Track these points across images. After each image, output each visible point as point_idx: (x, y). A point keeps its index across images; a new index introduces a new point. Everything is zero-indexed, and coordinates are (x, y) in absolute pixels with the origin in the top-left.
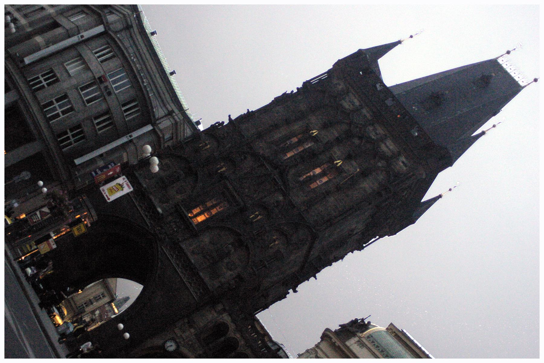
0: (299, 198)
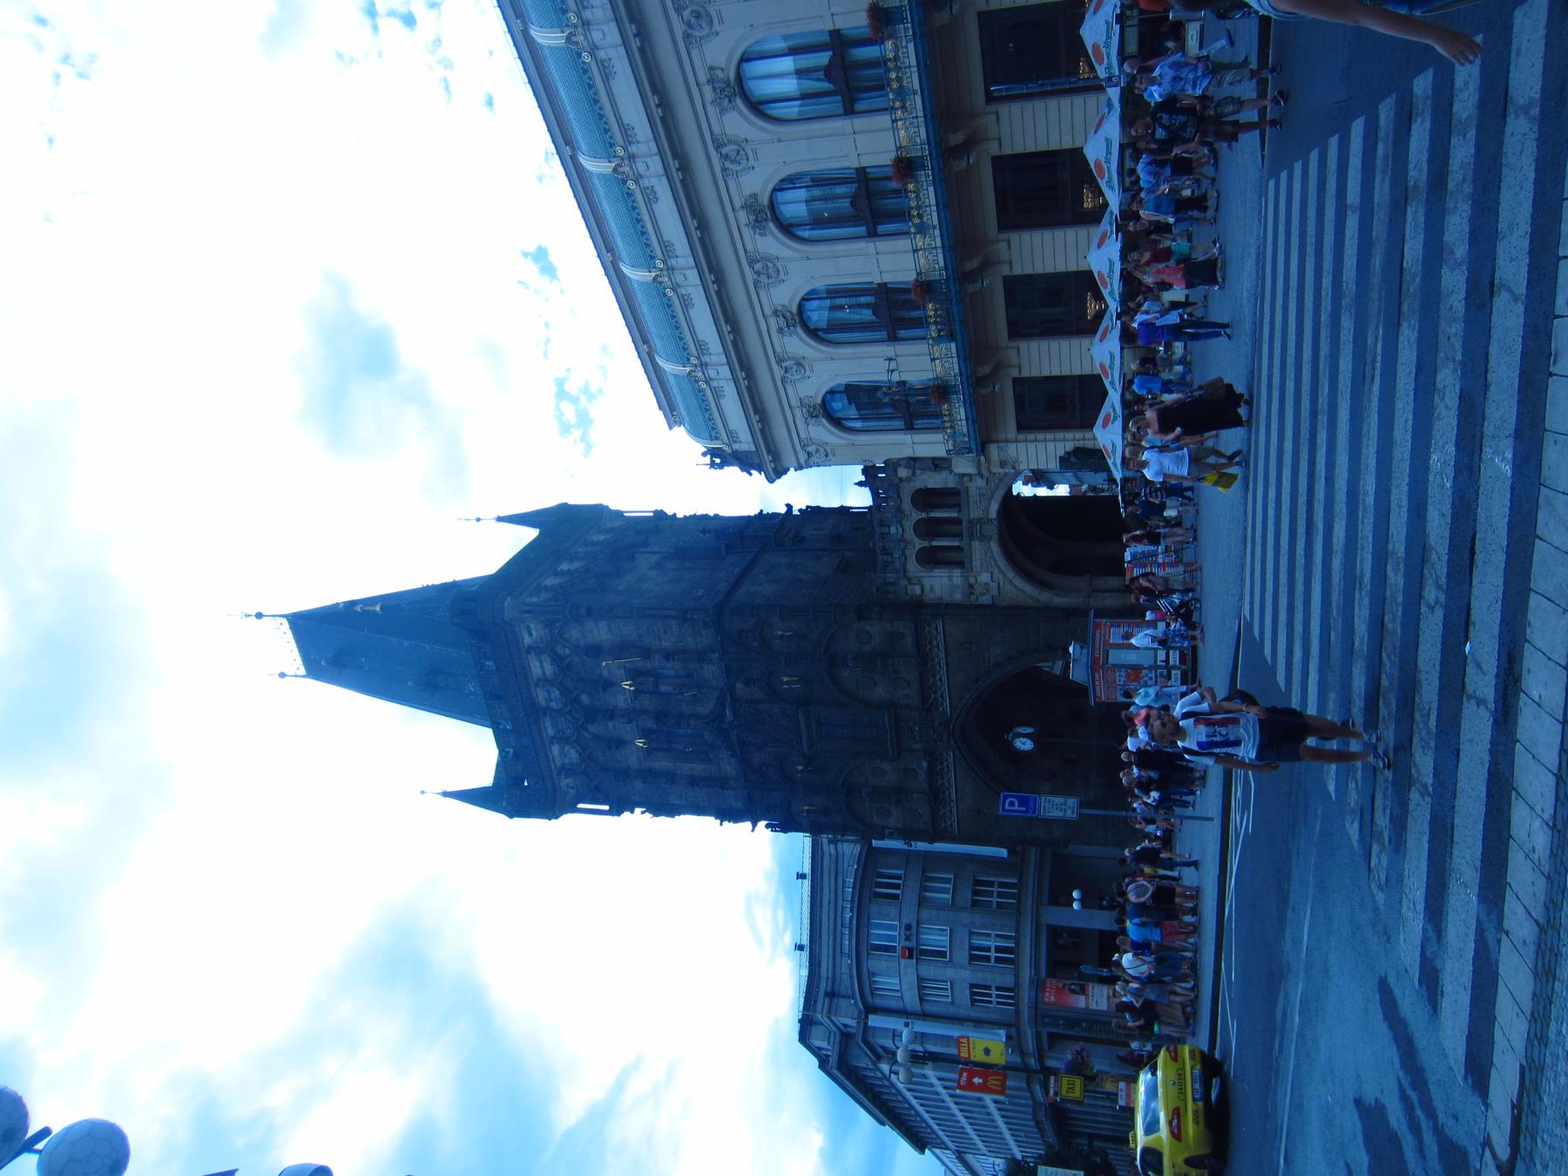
0: (711, 671)
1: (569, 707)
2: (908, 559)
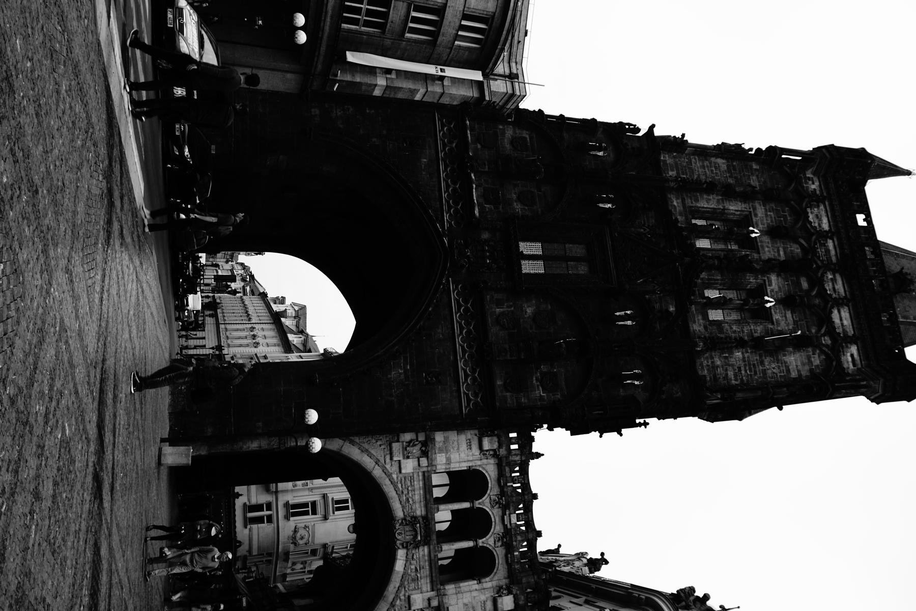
0: (697, 327)
1: (819, 275)
2: (496, 478)
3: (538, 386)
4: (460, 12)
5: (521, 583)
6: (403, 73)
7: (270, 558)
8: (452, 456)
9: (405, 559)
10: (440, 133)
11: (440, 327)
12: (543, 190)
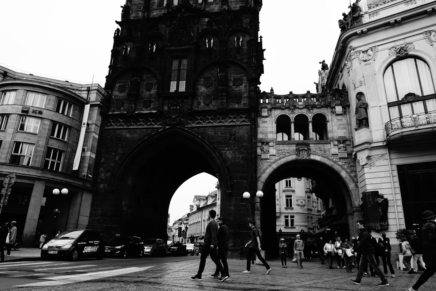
0: (216, 8)
3: (239, 88)
4: (55, 113)
5: (331, 102)
6: (85, 143)
7: (310, 217)
8: (270, 131)
9: (315, 155)
10: (115, 127)
11: (208, 132)
12: (145, 79)
